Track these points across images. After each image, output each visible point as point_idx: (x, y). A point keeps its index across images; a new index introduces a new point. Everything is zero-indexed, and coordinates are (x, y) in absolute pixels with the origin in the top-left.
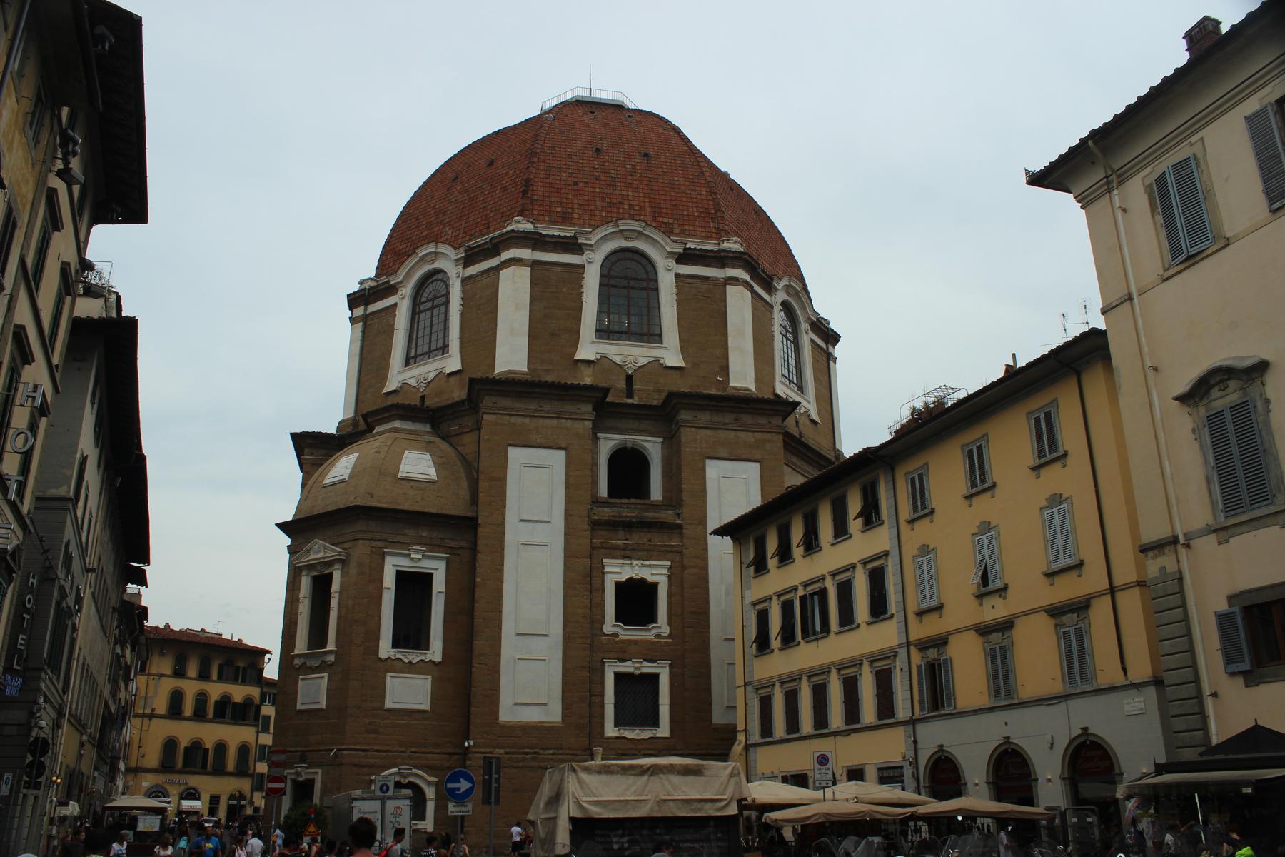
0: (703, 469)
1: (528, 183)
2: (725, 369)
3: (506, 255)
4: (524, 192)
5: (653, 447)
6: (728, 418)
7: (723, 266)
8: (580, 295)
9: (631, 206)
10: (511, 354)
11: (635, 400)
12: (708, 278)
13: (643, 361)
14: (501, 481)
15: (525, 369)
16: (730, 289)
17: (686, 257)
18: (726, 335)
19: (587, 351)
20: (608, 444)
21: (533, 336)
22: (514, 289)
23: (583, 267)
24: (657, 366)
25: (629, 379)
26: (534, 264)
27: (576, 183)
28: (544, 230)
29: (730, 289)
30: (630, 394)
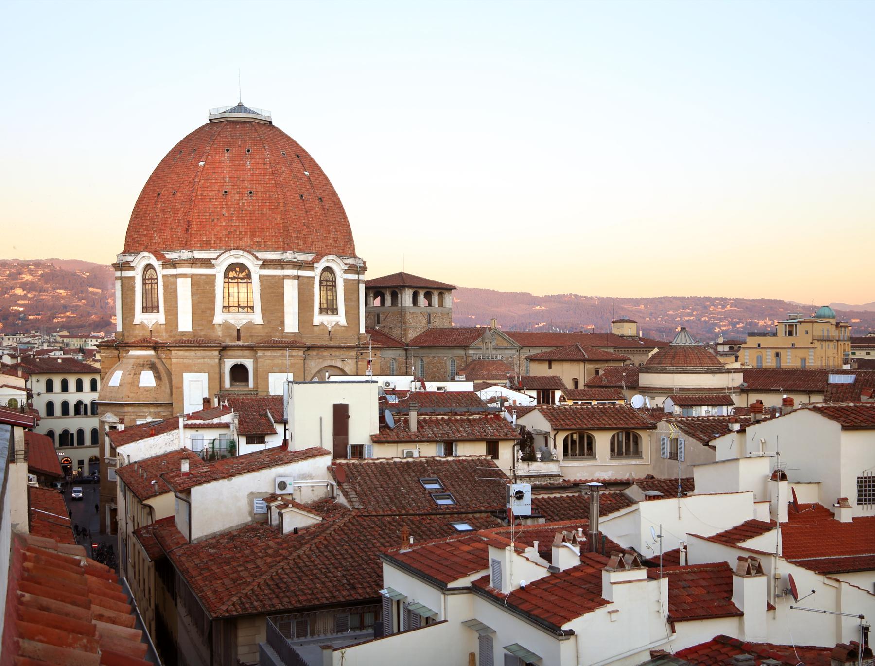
0: (268, 378)
1: (189, 223)
2: (282, 323)
3: (180, 271)
4: (187, 230)
5: (249, 363)
6: (278, 353)
7: (283, 269)
8: (214, 290)
9: (240, 232)
10: (185, 324)
11: (240, 343)
12: (275, 276)
13: (245, 322)
14: (181, 388)
15: (191, 330)
16: (286, 281)
17: (266, 264)
18: (283, 305)
19: (219, 317)
20: (229, 363)
21: (194, 313)
22: (184, 288)
23: (215, 275)
24: (250, 326)
25: (238, 330)
26: (192, 276)
27: (213, 220)
28: (198, 254)
29: (286, 281)
30: (239, 339)
